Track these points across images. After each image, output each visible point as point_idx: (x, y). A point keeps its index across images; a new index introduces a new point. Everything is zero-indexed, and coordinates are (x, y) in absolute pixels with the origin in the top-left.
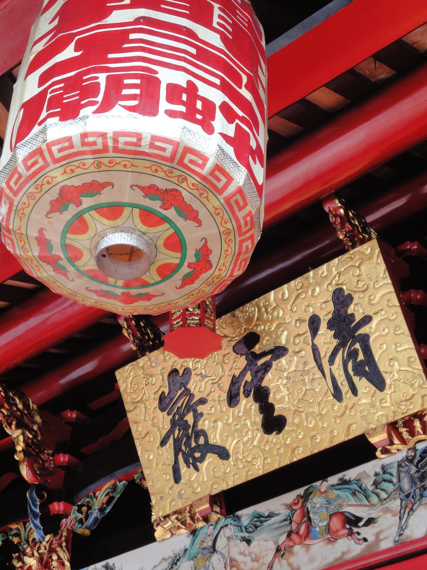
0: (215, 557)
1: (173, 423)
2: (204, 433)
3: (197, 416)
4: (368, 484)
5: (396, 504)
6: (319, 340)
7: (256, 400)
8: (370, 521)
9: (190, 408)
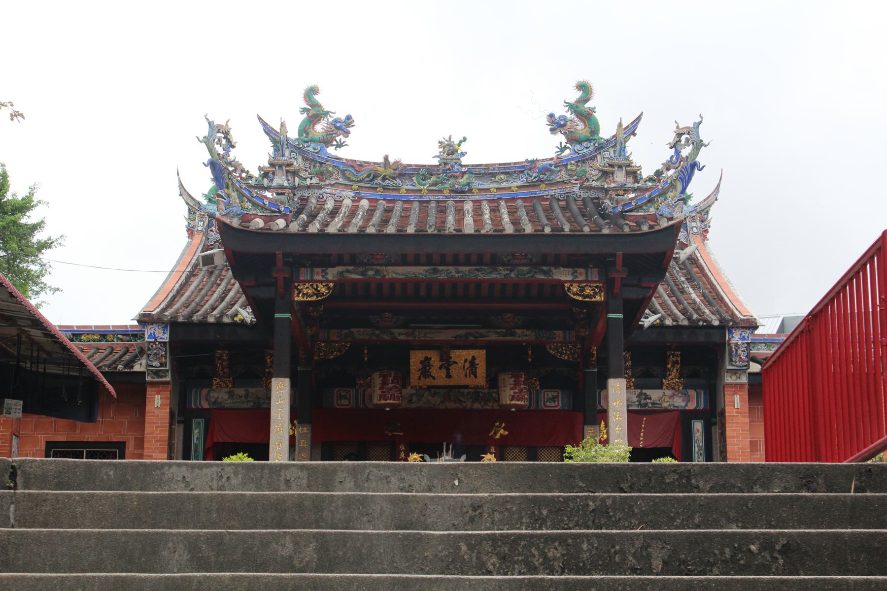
0: (424, 398)
1: (423, 368)
2: (430, 372)
3: (430, 368)
4: (465, 394)
5: (471, 400)
6: (466, 364)
7: (446, 370)
8: (464, 402)
9: (428, 366)
